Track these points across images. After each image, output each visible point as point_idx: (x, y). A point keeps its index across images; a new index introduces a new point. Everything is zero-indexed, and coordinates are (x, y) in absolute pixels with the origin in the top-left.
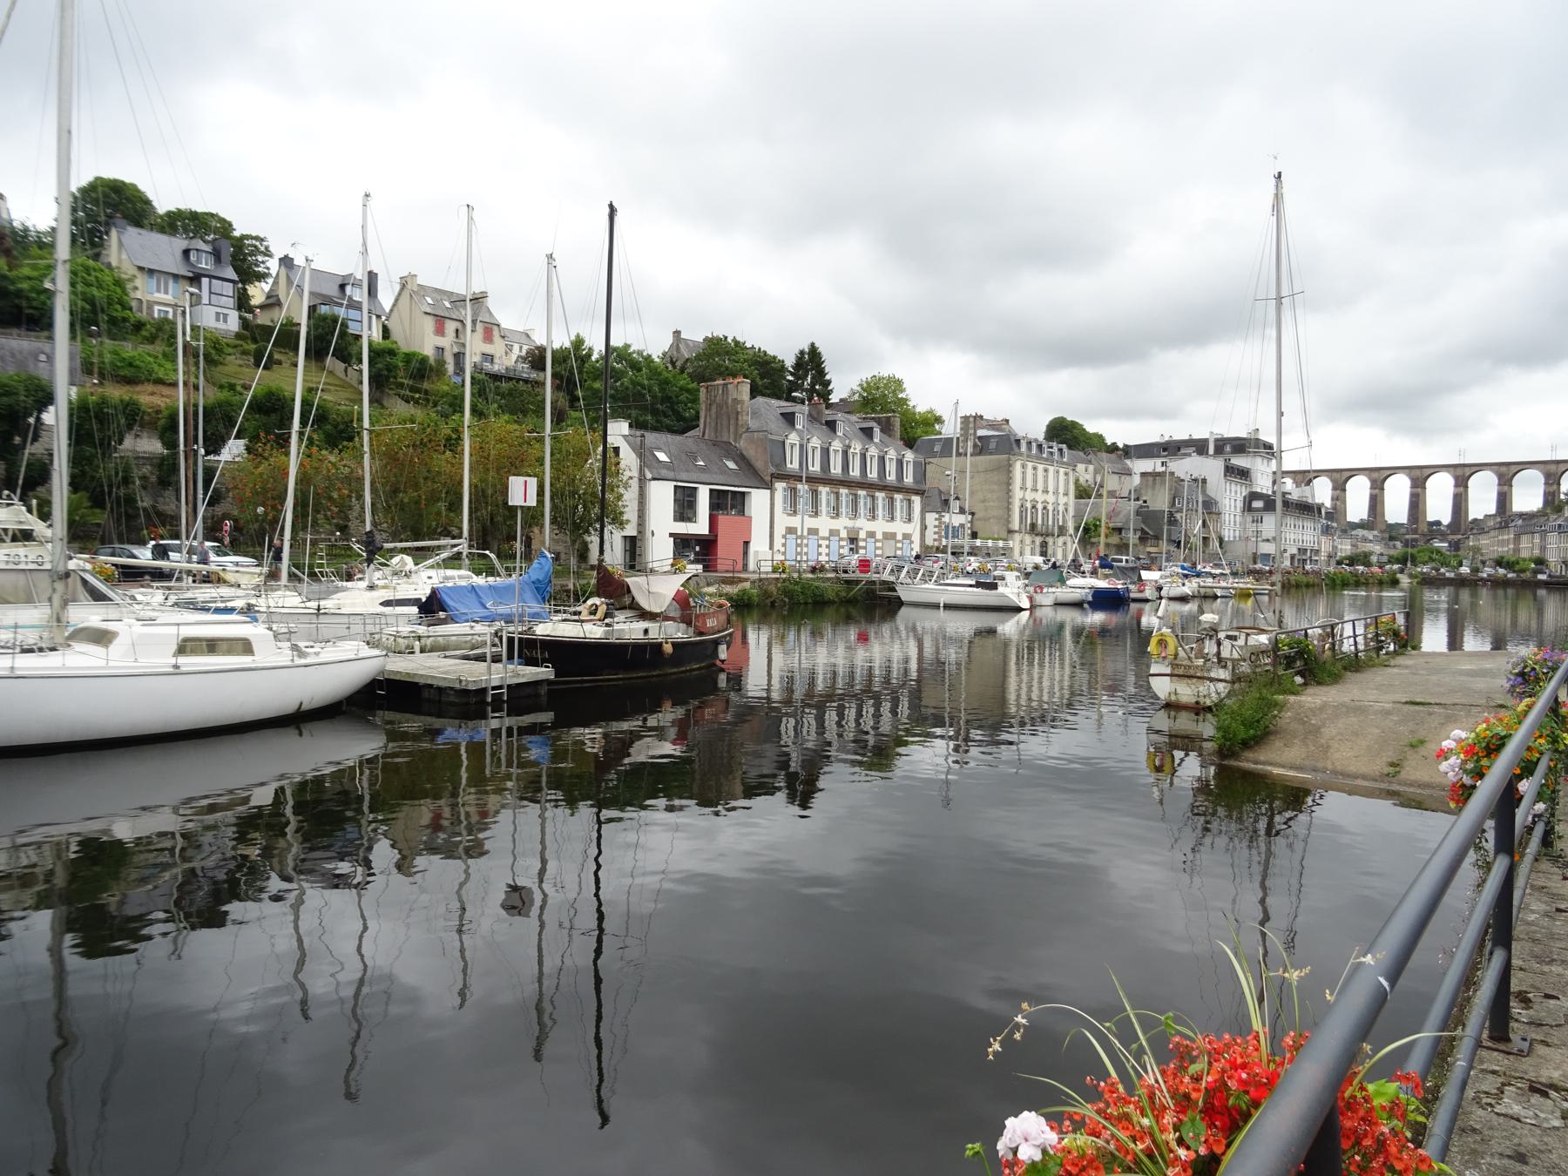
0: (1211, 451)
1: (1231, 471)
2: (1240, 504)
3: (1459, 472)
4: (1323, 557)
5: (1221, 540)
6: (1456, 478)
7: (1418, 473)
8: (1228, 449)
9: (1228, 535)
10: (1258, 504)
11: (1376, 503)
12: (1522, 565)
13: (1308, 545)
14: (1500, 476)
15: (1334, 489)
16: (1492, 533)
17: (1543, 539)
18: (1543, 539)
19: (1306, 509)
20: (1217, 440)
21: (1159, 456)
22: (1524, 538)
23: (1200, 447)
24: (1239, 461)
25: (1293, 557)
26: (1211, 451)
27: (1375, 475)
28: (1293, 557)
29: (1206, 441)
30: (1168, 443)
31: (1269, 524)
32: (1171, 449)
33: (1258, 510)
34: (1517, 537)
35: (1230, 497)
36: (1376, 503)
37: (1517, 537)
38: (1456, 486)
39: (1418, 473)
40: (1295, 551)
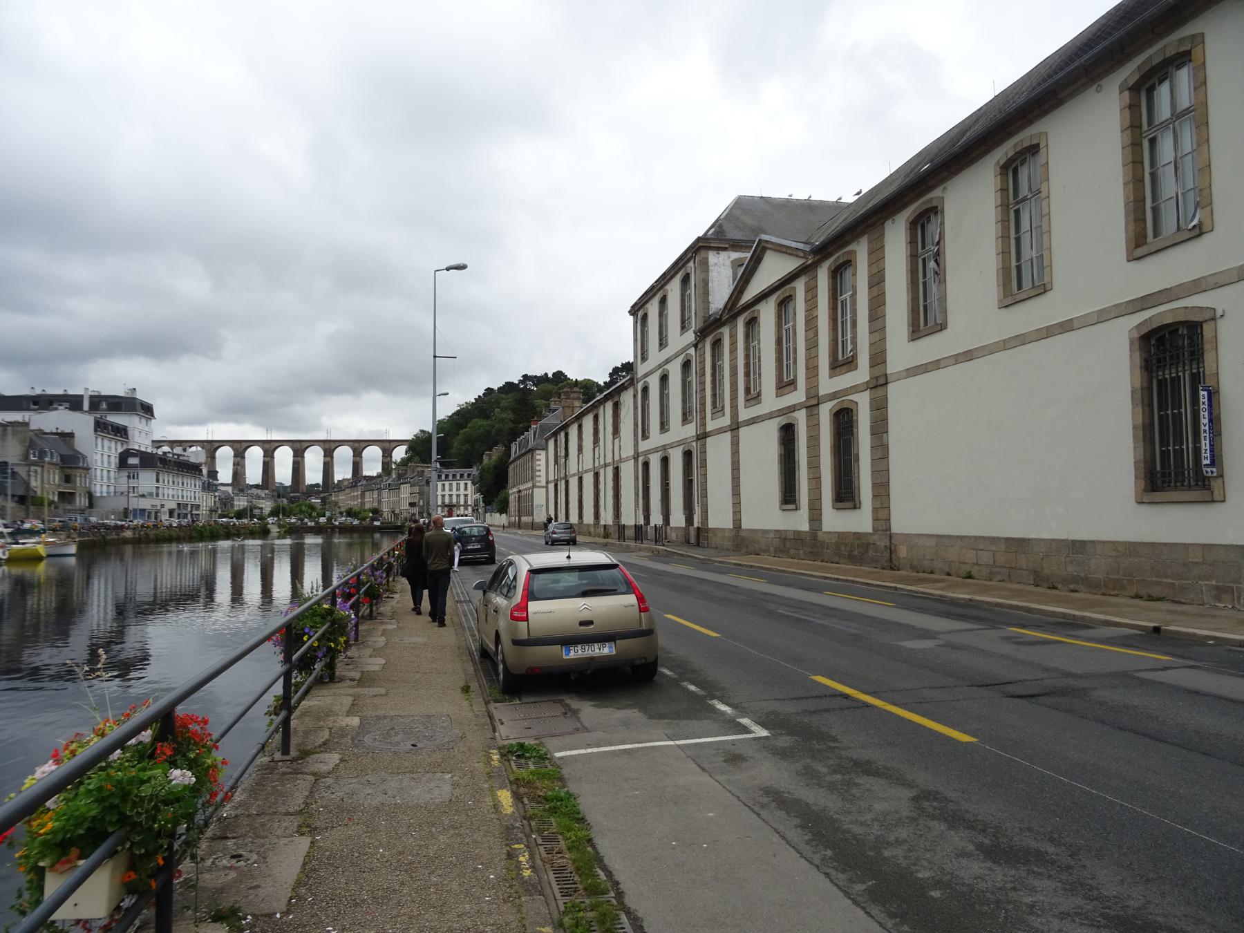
0: (86, 406)
1: (100, 426)
2: (114, 461)
3: (327, 446)
4: (204, 511)
5: (90, 496)
6: (325, 451)
7: (298, 445)
8: (104, 406)
9: (99, 490)
10: (133, 461)
11: (268, 468)
12: (363, 515)
13: (190, 501)
14: (354, 450)
15: (235, 456)
16: (347, 491)
17: (379, 495)
18: (379, 495)
19: (192, 469)
20: (91, 397)
21: (28, 409)
22: (367, 494)
23: (74, 403)
25: (171, 512)
26: (86, 406)
27: (267, 446)
28: (171, 512)
29: (82, 396)
30: (39, 396)
31: (146, 480)
32: (44, 402)
33: (134, 466)
34: (363, 493)
35: (101, 455)
36: (268, 468)
37: (363, 493)
38: (325, 456)
39: (298, 445)
40: (173, 505)
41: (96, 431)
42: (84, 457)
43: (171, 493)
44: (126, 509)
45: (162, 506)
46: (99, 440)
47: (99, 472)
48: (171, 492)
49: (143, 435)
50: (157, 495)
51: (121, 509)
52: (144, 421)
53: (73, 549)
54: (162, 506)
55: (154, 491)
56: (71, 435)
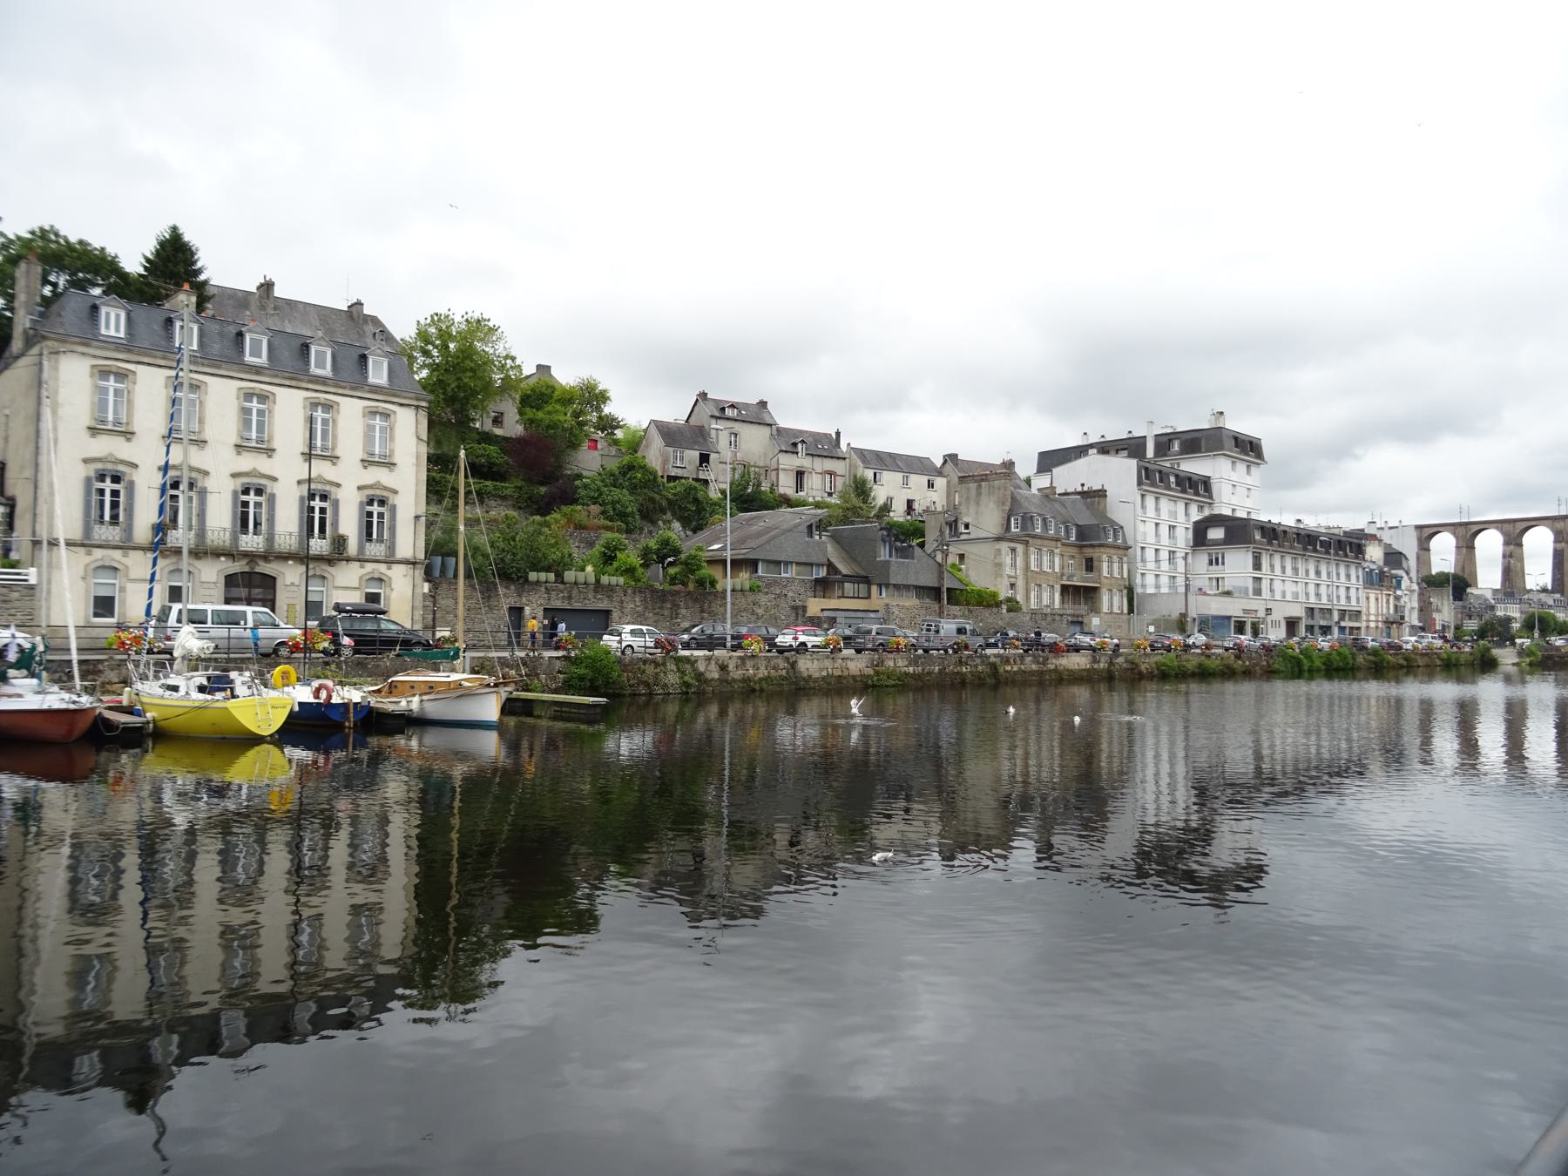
1: (1150, 477)
2: (1184, 537)
9: (1147, 584)
10: (1216, 534)
15: (1506, 543)
24: (1194, 466)
25: (1292, 624)
28: (1292, 624)
31: (1238, 564)
33: (1216, 543)
40: (1297, 611)
41: (1140, 483)
42: (1118, 529)
43: (1289, 592)
44: (1184, 616)
45: (1268, 611)
46: (1150, 500)
47: (1150, 554)
48: (1290, 588)
49: (1237, 491)
50: (1258, 592)
51: (1175, 615)
52: (1241, 467)
53: (489, 708)
54: (1268, 611)
55: (1250, 584)
56: (1101, 494)
